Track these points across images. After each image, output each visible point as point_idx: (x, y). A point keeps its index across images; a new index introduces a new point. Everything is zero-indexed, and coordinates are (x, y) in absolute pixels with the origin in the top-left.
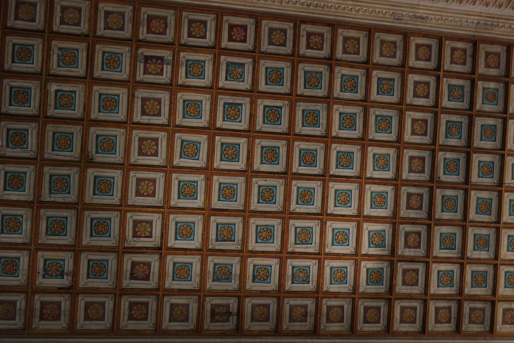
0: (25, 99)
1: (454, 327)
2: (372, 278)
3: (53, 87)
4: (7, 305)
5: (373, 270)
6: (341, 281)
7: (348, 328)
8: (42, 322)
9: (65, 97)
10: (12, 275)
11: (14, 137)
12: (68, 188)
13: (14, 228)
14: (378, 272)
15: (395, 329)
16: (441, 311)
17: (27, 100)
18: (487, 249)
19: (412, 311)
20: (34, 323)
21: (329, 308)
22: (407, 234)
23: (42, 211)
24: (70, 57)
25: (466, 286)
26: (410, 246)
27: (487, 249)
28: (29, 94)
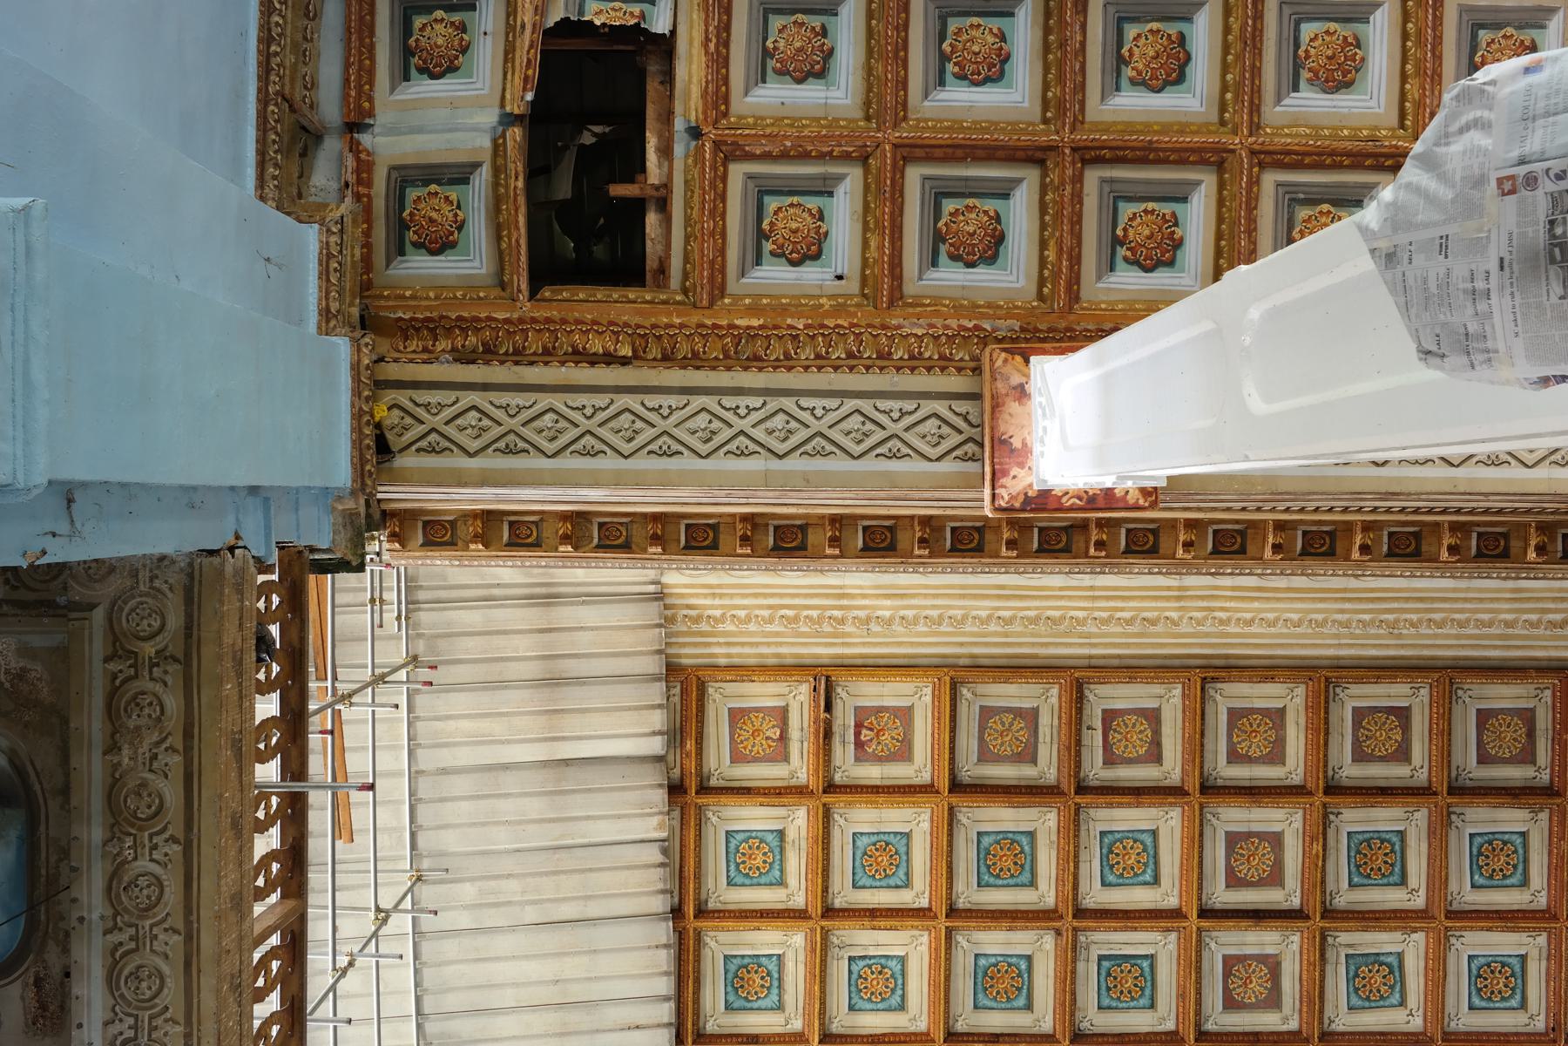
1: (1091, 697)
2: (1386, 855)
5: (1385, 881)
6: (1490, 843)
7: (1460, 693)
14: (1369, 876)
15: (1300, 690)
16: (1142, 751)
18: (982, 962)
19: (1242, 748)
21: (1527, 756)
22: (1273, 1001)
25: (1054, 838)
26: (1259, 962)
27: (982, 962)
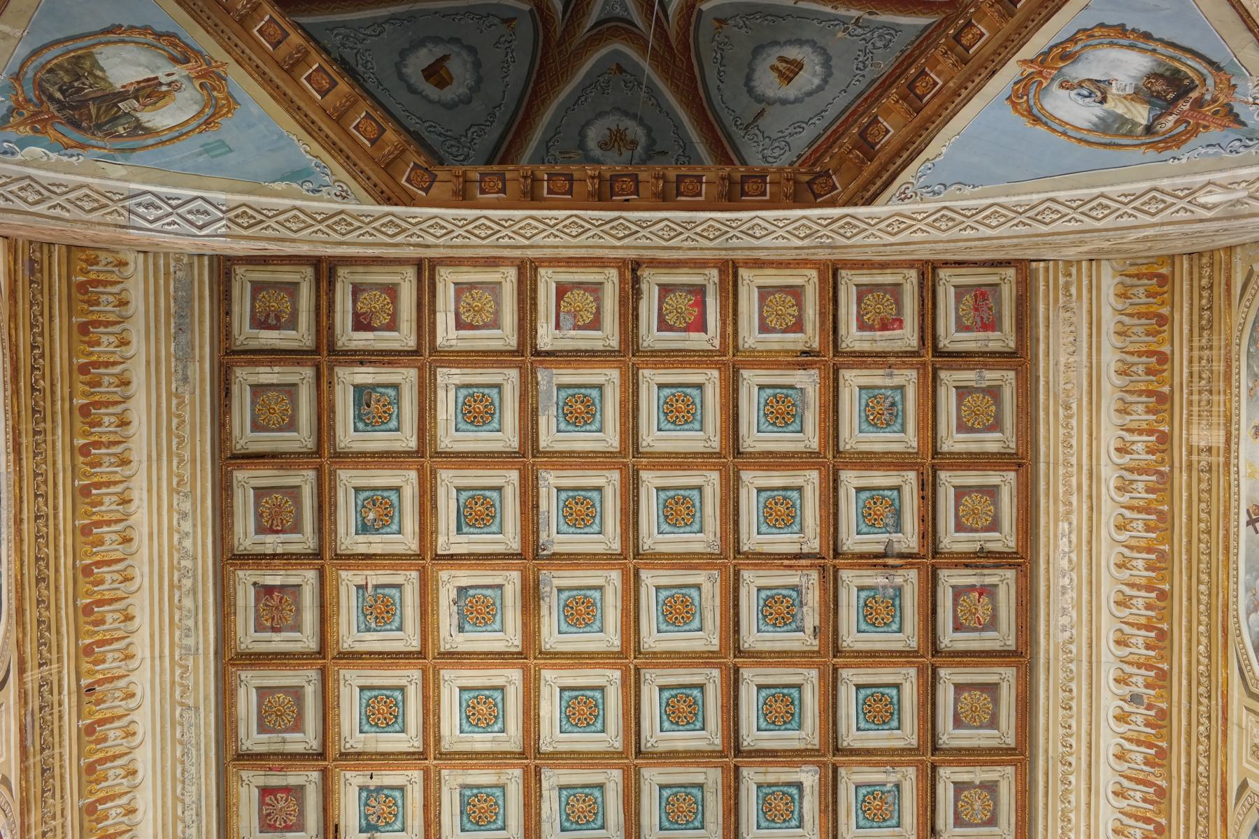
0: (776, 717)
3: (809, 777)
4: (293, 712)
8: (256, 791)
9: (787, 804)
10: (364, 717)
11: (685, 701)
12: (574, 826)
13: (474, 714)
17: (774, 723)
20: (251, 773)
23: (518, 772)
24: (881, 809)
28: (789, 726)
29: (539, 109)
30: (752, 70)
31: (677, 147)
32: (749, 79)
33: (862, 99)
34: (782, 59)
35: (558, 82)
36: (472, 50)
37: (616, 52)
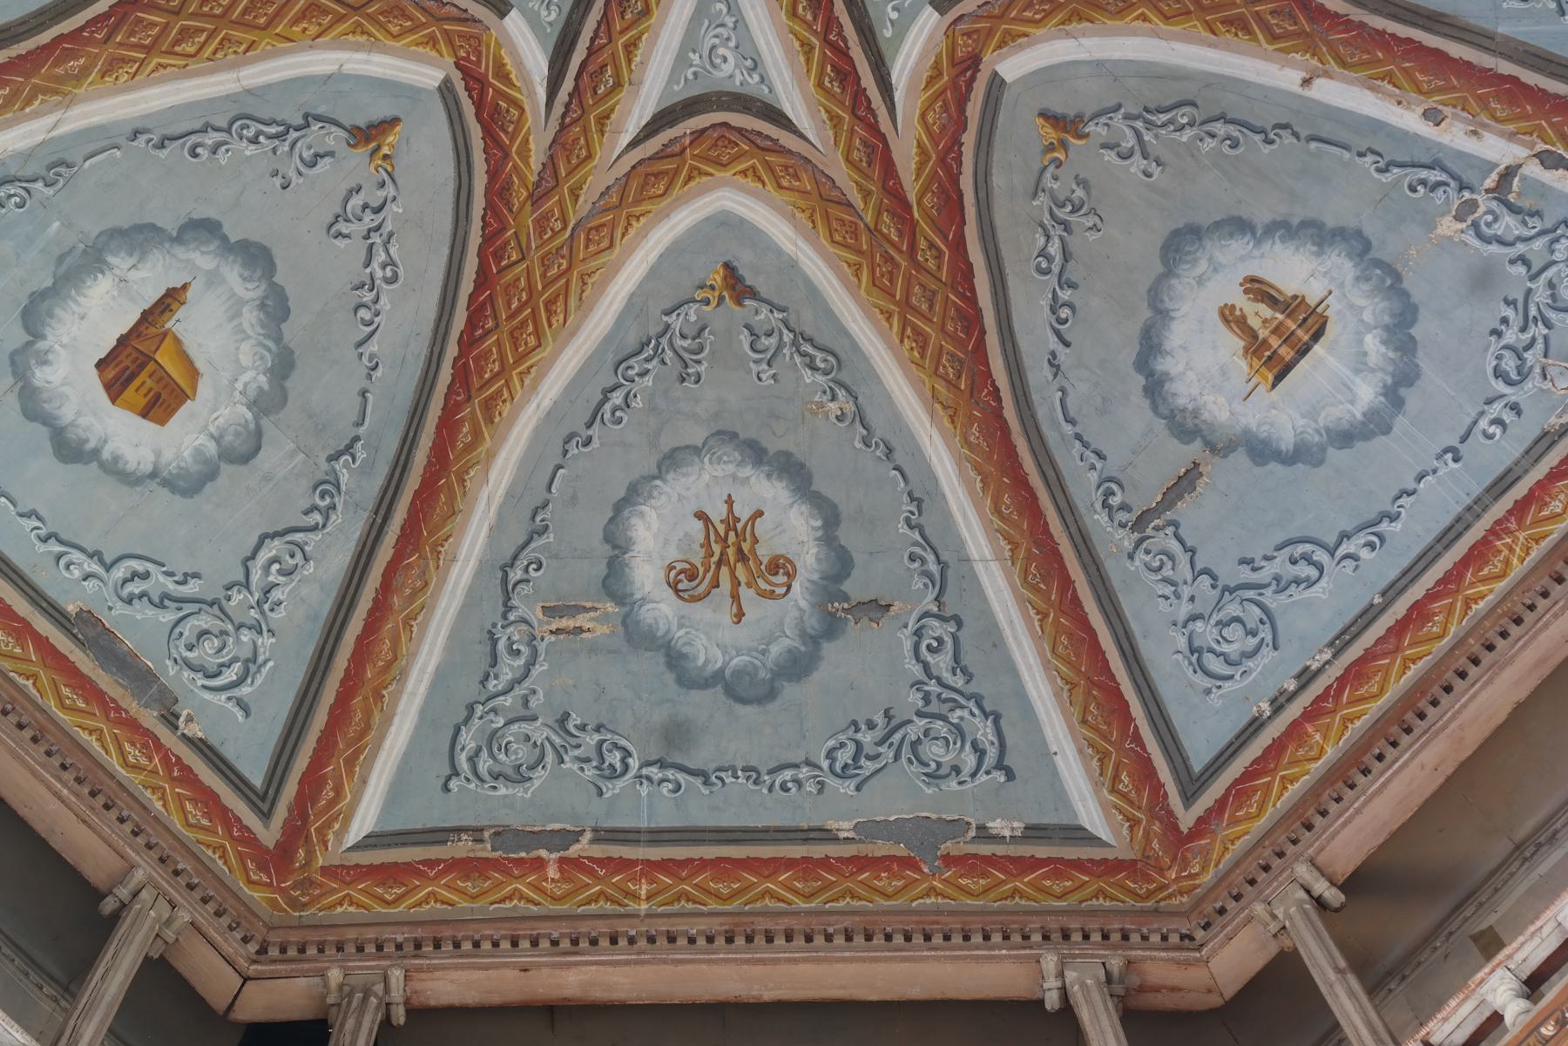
29: (477, 434)
30: (1161, 315)
31: (918, 583)
32: (1150, 346)
33: (1507, 502)
34: (1258, 289)
35: (538, 334)
36: (257, 257)
37: (726, 223)
